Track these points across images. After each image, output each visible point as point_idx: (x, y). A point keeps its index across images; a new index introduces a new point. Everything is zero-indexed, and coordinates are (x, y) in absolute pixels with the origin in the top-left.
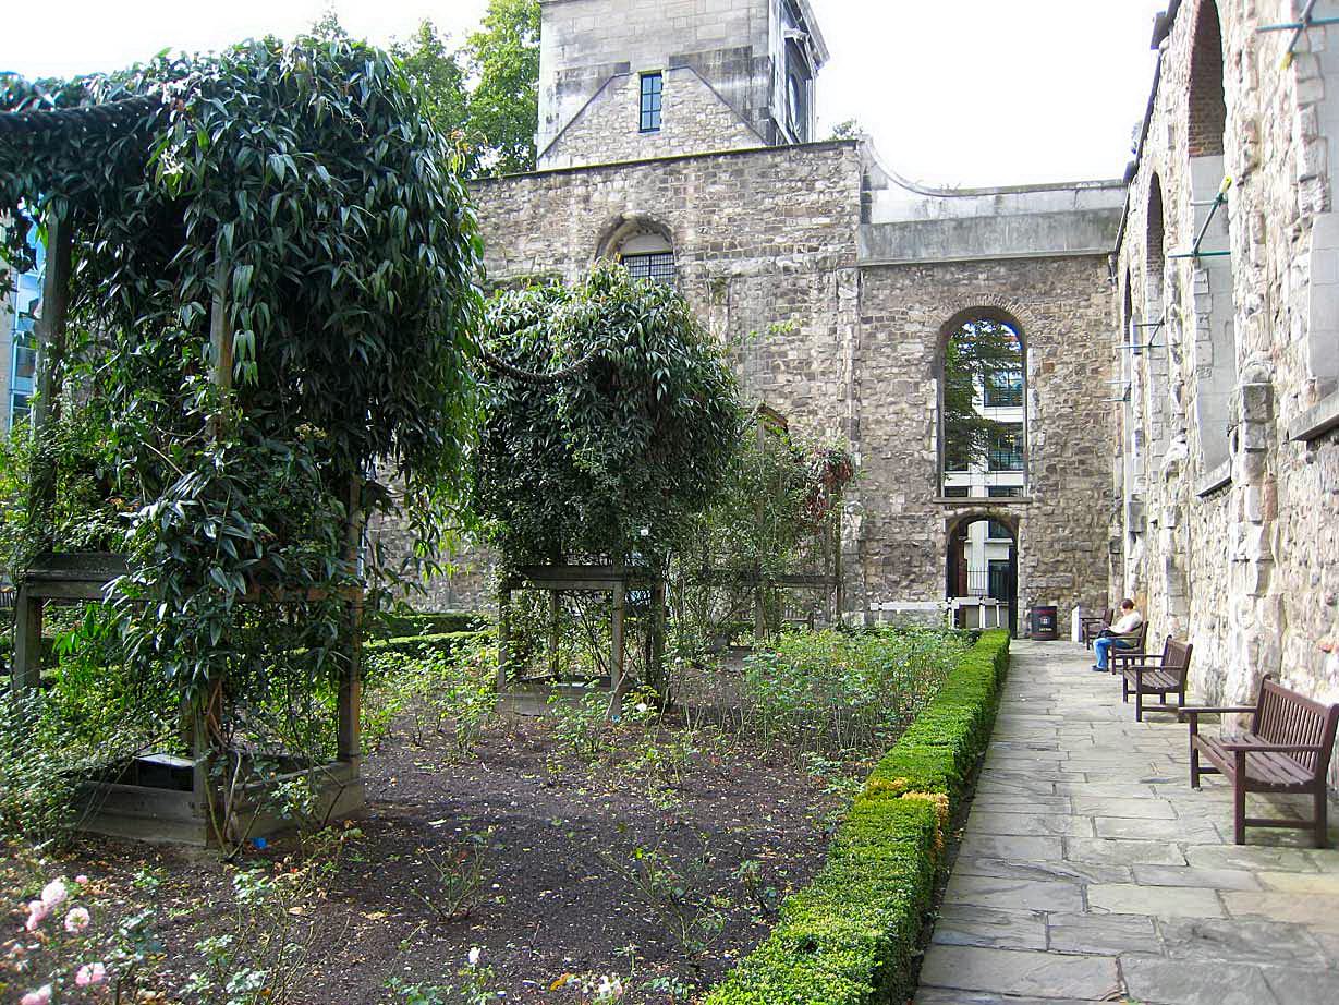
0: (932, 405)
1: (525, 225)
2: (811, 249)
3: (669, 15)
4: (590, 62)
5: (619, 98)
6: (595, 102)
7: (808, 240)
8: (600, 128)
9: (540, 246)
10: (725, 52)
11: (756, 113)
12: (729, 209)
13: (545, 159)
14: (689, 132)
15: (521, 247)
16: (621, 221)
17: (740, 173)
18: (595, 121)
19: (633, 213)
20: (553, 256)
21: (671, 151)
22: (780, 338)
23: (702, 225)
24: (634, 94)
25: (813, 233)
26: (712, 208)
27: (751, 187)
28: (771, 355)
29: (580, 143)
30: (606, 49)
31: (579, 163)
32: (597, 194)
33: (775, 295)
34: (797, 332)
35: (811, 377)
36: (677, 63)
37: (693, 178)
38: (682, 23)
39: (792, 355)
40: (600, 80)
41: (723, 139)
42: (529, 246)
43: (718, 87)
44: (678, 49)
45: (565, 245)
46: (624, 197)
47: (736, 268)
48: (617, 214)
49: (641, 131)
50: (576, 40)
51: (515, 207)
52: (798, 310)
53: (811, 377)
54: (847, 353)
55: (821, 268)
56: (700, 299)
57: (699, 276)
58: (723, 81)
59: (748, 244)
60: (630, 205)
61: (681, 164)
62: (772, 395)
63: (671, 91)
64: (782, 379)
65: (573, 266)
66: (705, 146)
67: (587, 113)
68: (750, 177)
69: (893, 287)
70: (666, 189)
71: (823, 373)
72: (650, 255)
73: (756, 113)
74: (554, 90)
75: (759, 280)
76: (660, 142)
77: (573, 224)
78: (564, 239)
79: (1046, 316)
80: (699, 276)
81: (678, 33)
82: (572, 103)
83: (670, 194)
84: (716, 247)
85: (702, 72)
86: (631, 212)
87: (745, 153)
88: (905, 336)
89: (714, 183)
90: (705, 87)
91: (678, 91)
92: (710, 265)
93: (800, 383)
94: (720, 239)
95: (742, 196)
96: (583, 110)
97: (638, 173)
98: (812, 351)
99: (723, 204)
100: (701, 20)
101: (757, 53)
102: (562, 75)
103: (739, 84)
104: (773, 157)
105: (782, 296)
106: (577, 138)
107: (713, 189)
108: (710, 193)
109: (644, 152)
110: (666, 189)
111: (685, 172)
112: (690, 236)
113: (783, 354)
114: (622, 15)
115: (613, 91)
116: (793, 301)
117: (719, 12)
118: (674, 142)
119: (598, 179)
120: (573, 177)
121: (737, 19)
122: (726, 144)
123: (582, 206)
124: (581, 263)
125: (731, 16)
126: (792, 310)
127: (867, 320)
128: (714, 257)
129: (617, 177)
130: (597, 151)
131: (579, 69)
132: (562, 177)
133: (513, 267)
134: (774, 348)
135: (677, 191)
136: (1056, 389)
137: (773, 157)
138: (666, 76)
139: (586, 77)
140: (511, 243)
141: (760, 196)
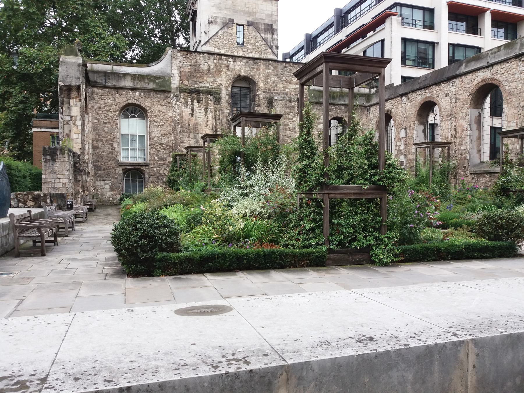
3: (247, 6)
4: (220, 15)
5: (230, 31)
6: (222, 30)
7: (295, 92)
8: (224, 40)
9: (212, 79)
10: (265, 24)
12: (273, 78)
13: (204, 46)
14: (254, 49)
15: (205, 78)
16: (239, 76)
17: (276, 67)
18: (222, 37)
19: (245, 74)
20: (216, 84)
21: (248, 54)
22: (288, 121)
23: (266, 82)
25: (296, 90)
26: (268, 77)
27: (280, 73)
28: (285, 125)
29: (217, 44)
31: (217, 51)
32: (231, 65)
33: (286, 107)
34: (292, 119)
37: (262, 66)
38: (251, 10)
39: (291, 125)
40: (223, 23)
41: (265, 53)
42: (208, 78)
43: (263, 35)
44: (250, 19)
45: (220, 81)
47: (276, 98)
48: (238, 74)
51: (202, 63)
52: (292, 113)
56: (265, 105)
57: (264, 98)
58: (264, 34)
59: (278, 90)
60: (242, 71)
61: (258, 61)
62: (285, 137)
63: (248, 33)
64: (288, 132)
65: (224, 89)
66: (259, 54)
68: (279, 68)
69: (317, 109)
70: (254, 68)
72: (240, 87)
73: (274, 48)
74: (207, 22)
75: (281, 102)
76: (244, 50)
80: (264, 98)
81: (250, 14)
83: (255, 70)
84: (269, 90)
85: (258, 29)
86: (243, 74)
87: (269, 60)
89: (269, 69)
90: (258, 34)
91: (252, 34)
94: (270, 87)
95: (277, 75)
96: (218, 32)
97: (245, 61)
98: (296, 125)
99: (271, 76)
100: (257, 11)
101: (274, 27)
102: (210, 17)
103: (269, 36)
104: (286, 64)
105: (288, 108)
106: (216, 41)
107: (268, 71)
108: (267, 72)
109: (239, 52)
110: (254, 68)
111: (259, 63)
112: (261, 85)
113: (288, 125)
114: (231, 2)
115: (228, 28)
116: (291, 110)
117: (263, 10)
118: (249, 51)
119: (231, 60)
120: (223, 57)
121: (269, 14)
122: (265, 55)
123: (226, 68)
124: (227, 88)
125: (266, 12)
126: (291, 112)
128: (269, 93)
129: (238, 60)
130: (223, 48)
131: (216, 17)
132: (218, 57)
134: (286, 123)
135: (257, 70)
137: (286, 64)
138: (246, 27)
139: (218, 20)
140: (200, 77)
141: (282, 76)
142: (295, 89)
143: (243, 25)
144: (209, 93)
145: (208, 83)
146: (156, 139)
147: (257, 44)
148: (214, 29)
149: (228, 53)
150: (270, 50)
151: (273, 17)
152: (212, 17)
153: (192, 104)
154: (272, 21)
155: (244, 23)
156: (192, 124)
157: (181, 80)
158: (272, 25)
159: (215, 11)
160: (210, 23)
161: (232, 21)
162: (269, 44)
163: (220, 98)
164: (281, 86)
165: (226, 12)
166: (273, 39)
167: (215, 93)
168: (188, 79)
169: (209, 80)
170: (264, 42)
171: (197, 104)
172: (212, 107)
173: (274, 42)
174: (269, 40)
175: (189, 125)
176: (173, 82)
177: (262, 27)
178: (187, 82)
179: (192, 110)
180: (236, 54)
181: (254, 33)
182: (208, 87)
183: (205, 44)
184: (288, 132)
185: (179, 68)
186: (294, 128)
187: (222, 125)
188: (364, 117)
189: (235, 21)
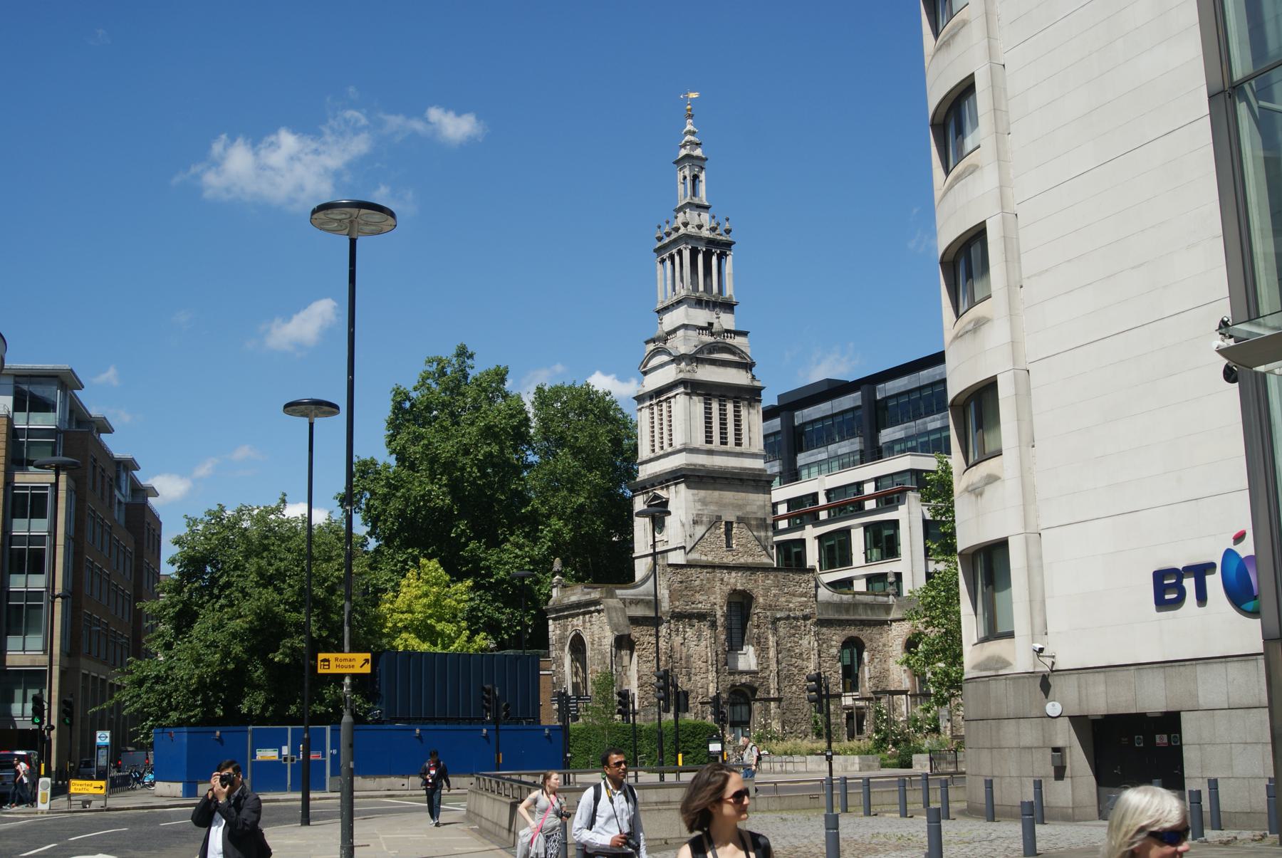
0: (840, 672)
1: (698, 588)
2: (802, 610)
4: (706, 512)
5: (718, 531)
9: (705, 597)
10: (756, 519)
11: (769, 547)
16: (735, 590)
19: (741, 588)
24: (722, 530)
26: (767, 590)
30: (712, 508)
31: (704, 558)
35: (803, 660)
36: (740, 520)
38: (740, 502)
40: (710, 522)
43: (755, 533)
44: (739, 514)
45: (715, 599)
46: (737, 581)
49: (727, 547)
50: (699, 500)
53: (803, 660)
54: (816, 652)
55: (806, 618)
66: (751, 558)
67: (706, 535)
71: (807, 659)
73: (769, 547)
77: (718, 591)
78: (714, 596)
79: (871, 640)
81: (739, 507)
82: (700, 530)
84: (770, 606)
85: (749, 527)
86: (739, 587)
88: (832, 646)
92: (768, 613)
93: (800, 662)
96: (704, 535)
103: (763, 534)
112: (761, 600)
113: (794, 651)
116: (796, 630)
117: (754, 501)
119: (725, 571)
124: (721, 607)
125: (758, 503)
127: (820, 639)
128: (769, 610)
133: (693, 606)
135: (755, 581)
136: (875, 667)
138: (735, 525)
139: (705, 519)
140: (693, 595)
142: (800, 602)
143: (731, 523)
144: (701, 617)
145: (702, 603)
146: (645, 678)
147: (749, 545)
148: (700, 530)
149: (717, 561)
150: (764, 552)
151: (767, 508)
152: (697, 515)
153: (685, 632)
154: (765, 514)
155: (732, 519)
156: (684, 655)
157: (671, 601)
158: (765, 519)
159: (700, 508)
160: (695, 522)
161: (719, 518)
162: (763, 544)
163: (715, 622)
164: (784, 599)
165: (712, 508)
166: (767, 538)
167: (710, 615)
168: (678, 600)
169: (701, 598)
170: (757, 543)
171: (688, 630)
172: (707, 633)
173: (769, 540)
174: (763, 538)
175: (681, 659)
176: (663, 605)
177: (753, 522)
178: (677, 603)
179: (685, 639)
180: (725, 560)
181: (746, 532)
182: (701, 608)
183: (690, 551)
184: (794, 660)
185: (669, 587)
186: (801, 654)
187: (717, 655)
188: (885, 635)
189: (723, 518)
